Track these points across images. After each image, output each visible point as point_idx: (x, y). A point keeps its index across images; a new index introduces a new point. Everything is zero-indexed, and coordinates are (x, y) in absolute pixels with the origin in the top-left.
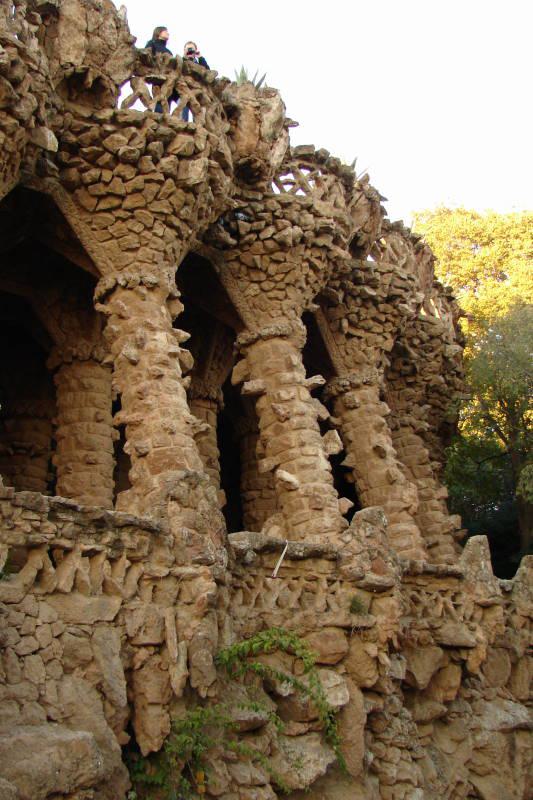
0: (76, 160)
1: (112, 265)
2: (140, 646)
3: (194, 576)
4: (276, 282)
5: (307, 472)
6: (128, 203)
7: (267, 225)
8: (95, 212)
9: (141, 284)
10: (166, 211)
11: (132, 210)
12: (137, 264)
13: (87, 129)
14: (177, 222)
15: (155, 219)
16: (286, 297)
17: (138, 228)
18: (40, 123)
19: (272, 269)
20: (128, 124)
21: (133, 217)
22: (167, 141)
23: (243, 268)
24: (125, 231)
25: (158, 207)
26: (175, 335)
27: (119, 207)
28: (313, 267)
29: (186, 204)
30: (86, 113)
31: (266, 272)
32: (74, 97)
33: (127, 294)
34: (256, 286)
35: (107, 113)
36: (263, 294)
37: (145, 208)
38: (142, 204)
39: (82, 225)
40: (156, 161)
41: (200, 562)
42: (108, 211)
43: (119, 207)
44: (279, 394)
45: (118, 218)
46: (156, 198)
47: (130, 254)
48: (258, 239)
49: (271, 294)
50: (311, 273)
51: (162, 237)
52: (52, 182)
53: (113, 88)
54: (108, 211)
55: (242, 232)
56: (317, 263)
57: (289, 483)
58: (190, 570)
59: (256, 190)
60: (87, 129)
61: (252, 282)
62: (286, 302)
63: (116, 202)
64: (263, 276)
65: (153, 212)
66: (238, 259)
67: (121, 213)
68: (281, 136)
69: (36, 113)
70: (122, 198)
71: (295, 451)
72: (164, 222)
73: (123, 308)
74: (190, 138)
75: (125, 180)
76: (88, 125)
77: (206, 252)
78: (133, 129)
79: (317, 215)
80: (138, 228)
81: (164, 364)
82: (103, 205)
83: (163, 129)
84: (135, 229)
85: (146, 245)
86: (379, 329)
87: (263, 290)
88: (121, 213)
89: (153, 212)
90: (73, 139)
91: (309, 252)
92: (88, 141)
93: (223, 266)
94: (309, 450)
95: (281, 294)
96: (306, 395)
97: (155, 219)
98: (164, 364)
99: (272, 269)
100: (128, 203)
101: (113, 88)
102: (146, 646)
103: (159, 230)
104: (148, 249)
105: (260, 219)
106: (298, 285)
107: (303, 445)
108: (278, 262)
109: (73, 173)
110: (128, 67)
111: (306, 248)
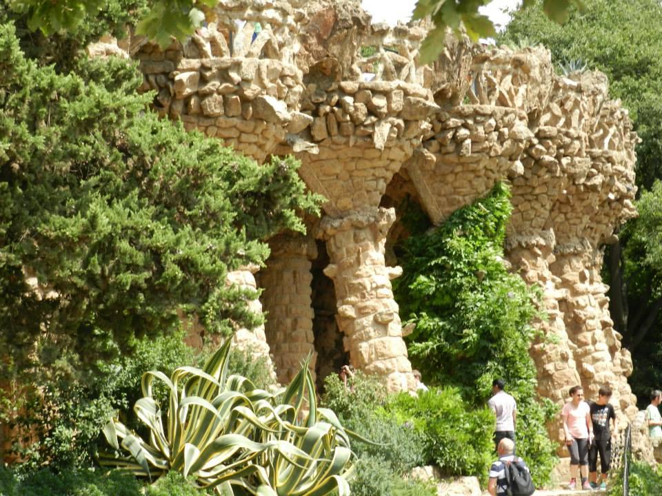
5: (599, 364)
6: (537, 191)
9: (537, 246)
11: (537, 195)
12: (531, 229)
17: (537, 206)
19: (577, 204)
20: (546, 138)
21: (537, 199)
24: (529, 207)
26: (553, 280)
33: (526, 253)
36: (567, 223)
37: (546, 193)
42: (522, 195)
43: (531, 193)
44: (577, 302)
47: (528, 223)
49: (572, 222)
54: (522, 195)
61: (561, 213)
63: (530, 190)
67: (530, 197)
70: (534, 188)
71: (590, 347)
73: (525, 264)
75: (539, 177)
78: (550, 142)
80: (537, 206)
83: (567, 140)
85: (539, 216)
86: (606, 220)
88: (530, 197)
94: (598, 346)
95: (577, 221)
99: (577, 204)
100: (537, 191)
104: (539, 219)
107: (594, 342)
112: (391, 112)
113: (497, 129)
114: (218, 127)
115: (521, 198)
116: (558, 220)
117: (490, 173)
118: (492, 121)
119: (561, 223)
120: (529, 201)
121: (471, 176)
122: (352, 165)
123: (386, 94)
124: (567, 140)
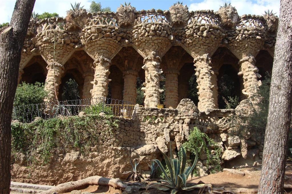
0: (182, 38)
1: (195, 56)
2: (175, 132)
3: (185, 119)
4: (243, 48)
6: (194, 44)
7: (237, 36)
8: (188, 47)
10: (202, 43)
11: (195, 45)
13: (182, 32)
14: (206, 44)
15: (200, 45)
16: (246, 51)
18: (169, 35)
22: (198, 29)
23: (234, 47)
24: (195, 49)
25: (200, 43)
27: (192, 45)
28: (251, 42)
29: (206, 40)
30: (181, 29)
31: (239, 46)
32: (178, 26)
34: (238, 50)
35: (185, 27)
37: (198, 43)
38: (196, 43)
39: (187, 50)
40: (197, 34)
41: (186, 116)
43: (192, 45)
45: (193, 47)
46: (199, 41)
48: (235, 40)
50: (252, 44)
51: (203, 48)
52: (179, 43)
53: (185, 22)
55: (230, 40)
56: (253, 41)
57: (246, 95)
58: (184, 117)
59: (232, 29)
60: (182, 32)
62: (247, 52)
64: (239, 48)
65: (199, 44)
66: (232, 45)
67: (193, 46)
68: (234, 16)
69: (167, 33)
72: (203, 45)
74: (203, 27)
76: (182, 31)
77: (224, 46)
79: (248, 31)
81: (204, 75)
82: (189, 45)
84: (197, 48)
87: (240, 51)
88: (193, 46)
89: (199, 44)
90: (180, 34)
91: (249, 40)
92: (183, 34)
93: (230, 47)
96: (253, 73)
97: (200, 45)
98: (204, 75)
99: (241, 46)
100: (194, 44)
101: (185, 22)
102: (176, 132)
103: (202, 47)
105: (234, 35)
106: (249, 47)
108: (242, 44)
109: (182, 41)
110: (188, 17)
111: (248, 39)
112: (92, 33)
113: (144, 29)
114: (43, 47)
115: (191, 47)
116: (237, 52)
117: (149, 41)
118: (142, 28)
119: (239, 52)
120: (194, 47)
121: (145, 43)
122: (92, 48)
123: (90, 29)
124: (197, 27)
